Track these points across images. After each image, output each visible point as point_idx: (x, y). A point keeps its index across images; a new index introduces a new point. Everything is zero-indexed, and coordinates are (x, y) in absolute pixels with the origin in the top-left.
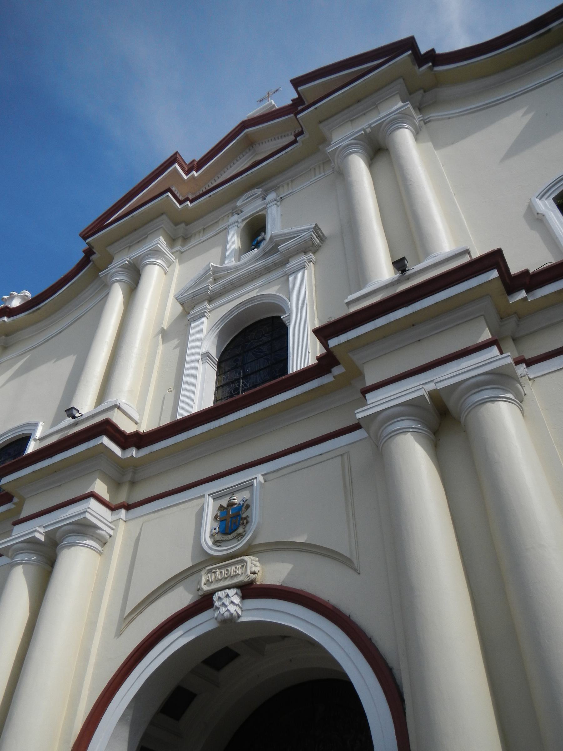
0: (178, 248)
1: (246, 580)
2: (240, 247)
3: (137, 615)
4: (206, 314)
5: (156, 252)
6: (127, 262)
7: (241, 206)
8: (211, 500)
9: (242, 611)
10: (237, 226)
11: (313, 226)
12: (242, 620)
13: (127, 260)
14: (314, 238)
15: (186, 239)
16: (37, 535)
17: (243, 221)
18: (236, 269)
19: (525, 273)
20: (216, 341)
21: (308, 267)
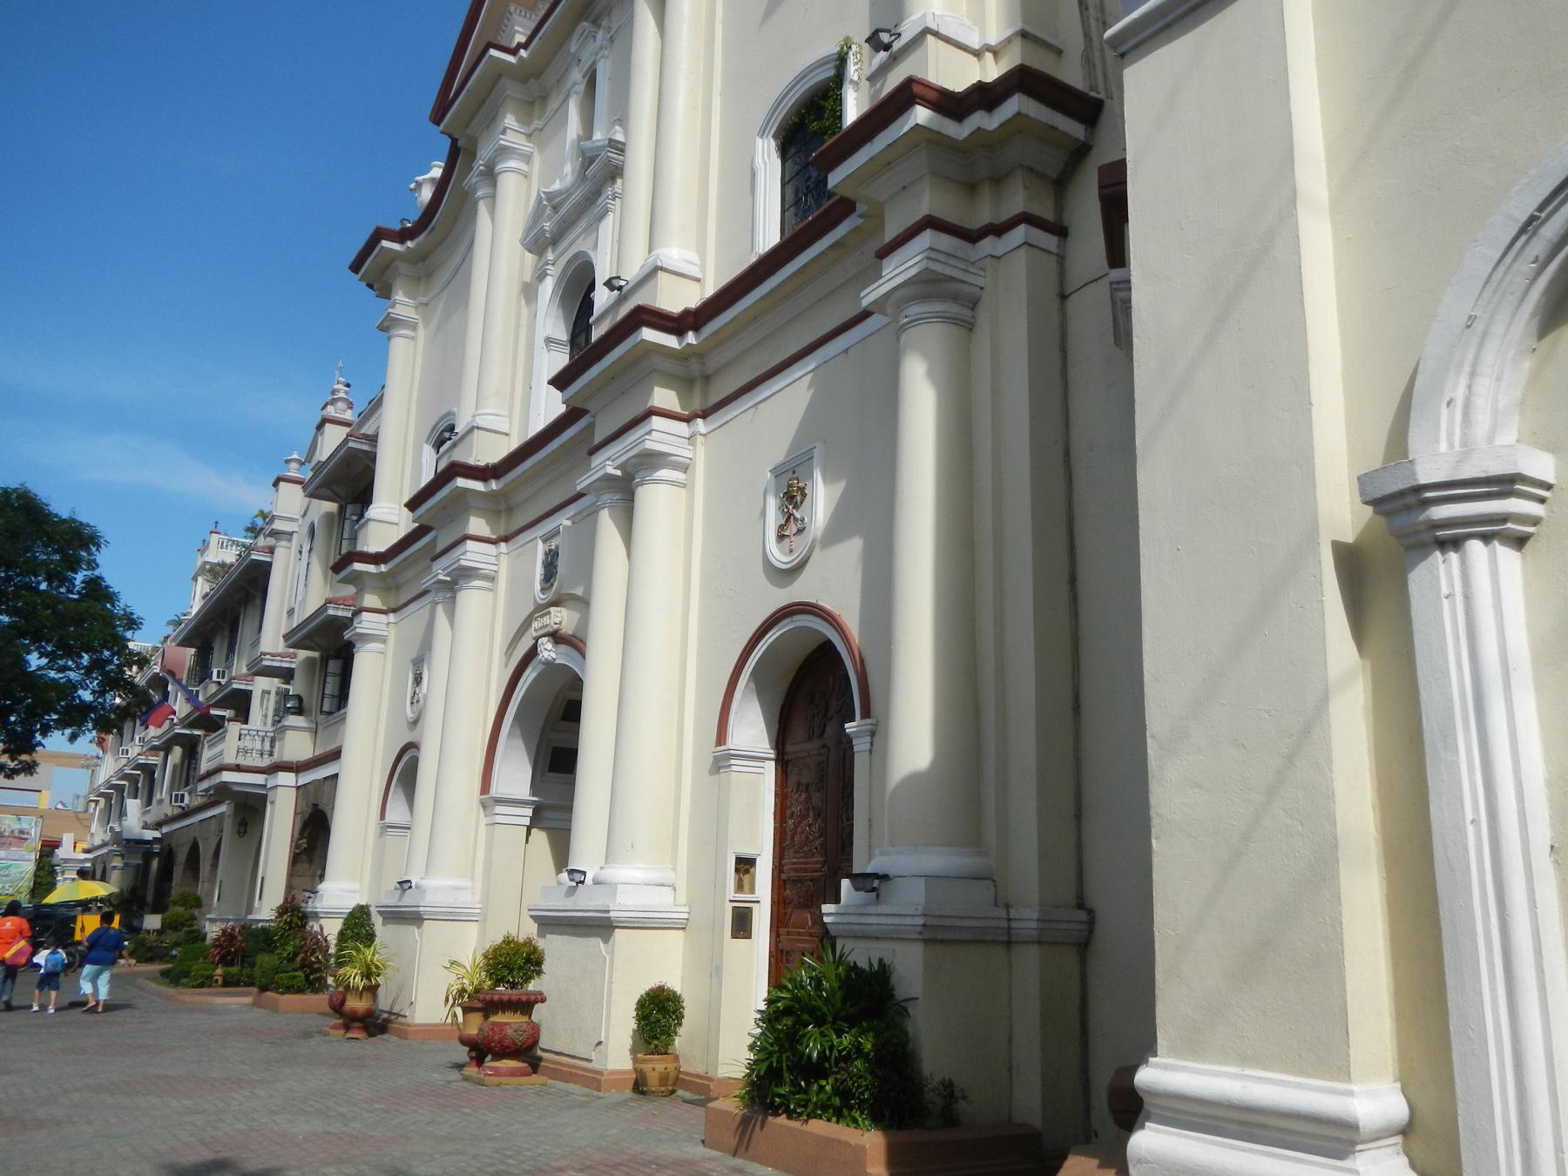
0: (537, 124)
1: (551, 630)
2: (581, 134)
3: (513, 651)
4: (548, 272)
5: (505, 152)
6: (481, 168)
7: (576, 52)
8: (540, 543)
9: (557, 654)
10: (576, 93)
11: (607, 142)
12: (557, 662)
13: (481, 165)
14: (614, 159)
15: (544, 99)
16: (441, 577)
17: (584, 77)
18: (568, 192)
19: (687, 312)
20: (560, 312)
21: (613, 207)
